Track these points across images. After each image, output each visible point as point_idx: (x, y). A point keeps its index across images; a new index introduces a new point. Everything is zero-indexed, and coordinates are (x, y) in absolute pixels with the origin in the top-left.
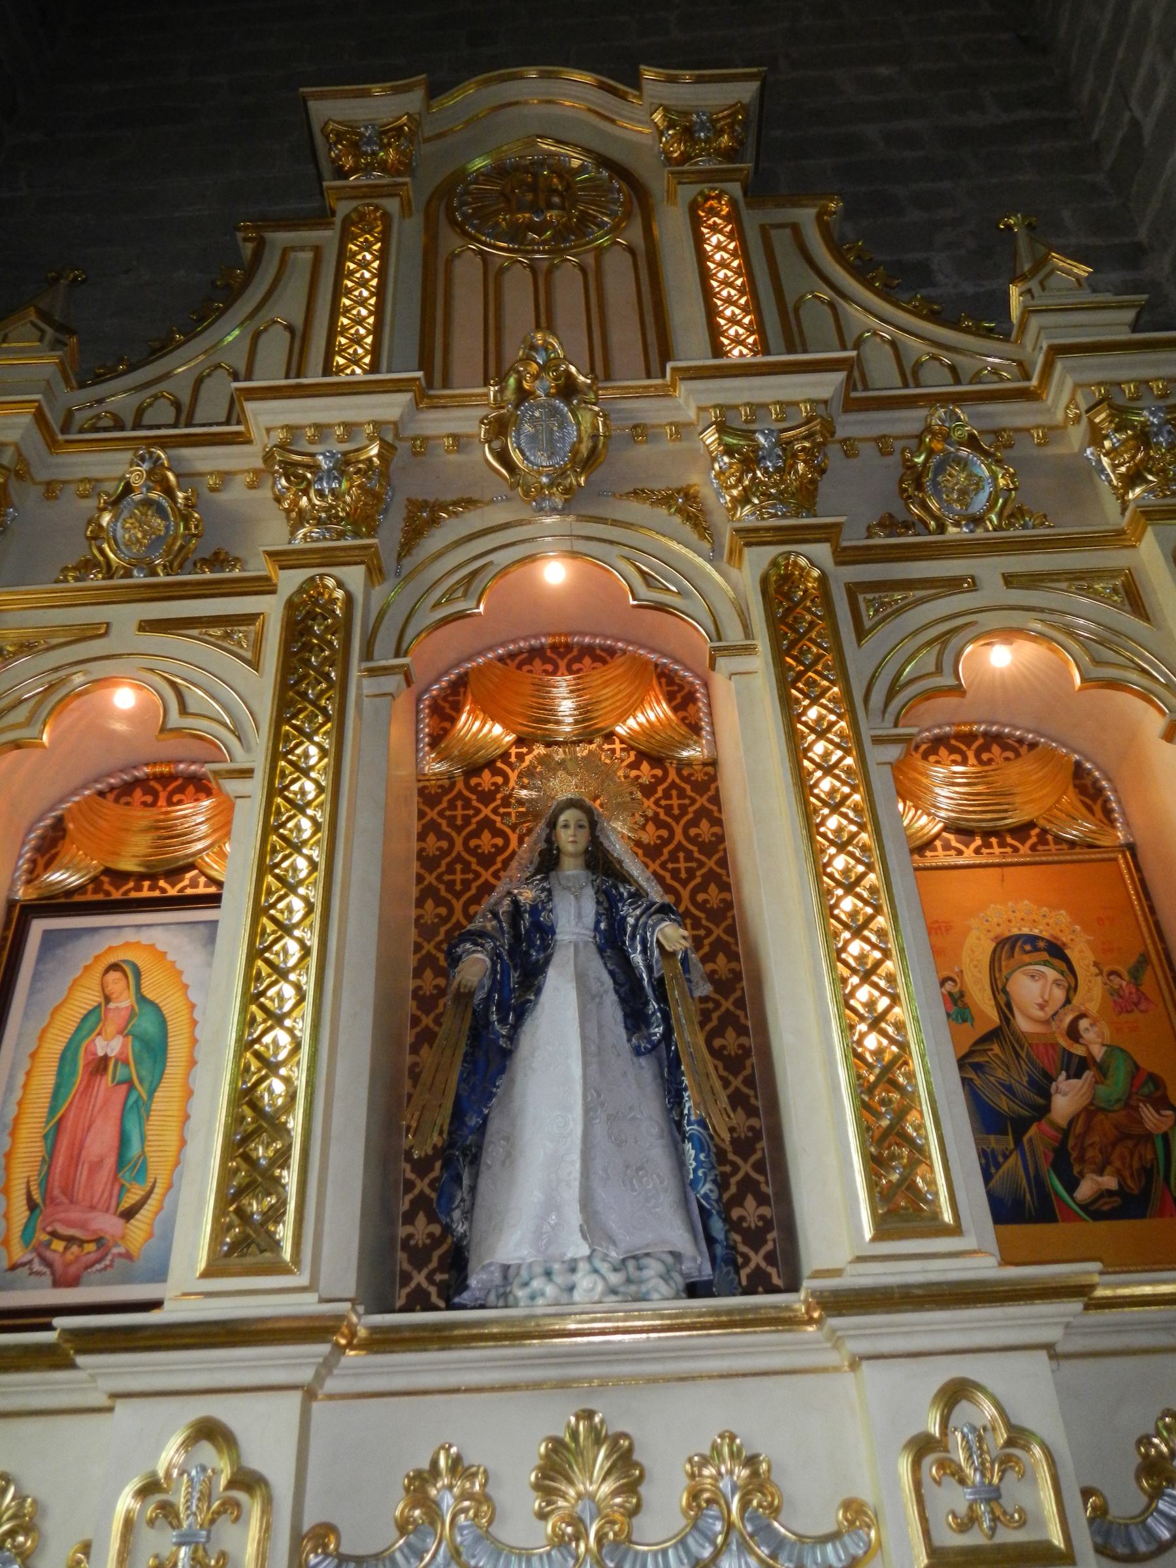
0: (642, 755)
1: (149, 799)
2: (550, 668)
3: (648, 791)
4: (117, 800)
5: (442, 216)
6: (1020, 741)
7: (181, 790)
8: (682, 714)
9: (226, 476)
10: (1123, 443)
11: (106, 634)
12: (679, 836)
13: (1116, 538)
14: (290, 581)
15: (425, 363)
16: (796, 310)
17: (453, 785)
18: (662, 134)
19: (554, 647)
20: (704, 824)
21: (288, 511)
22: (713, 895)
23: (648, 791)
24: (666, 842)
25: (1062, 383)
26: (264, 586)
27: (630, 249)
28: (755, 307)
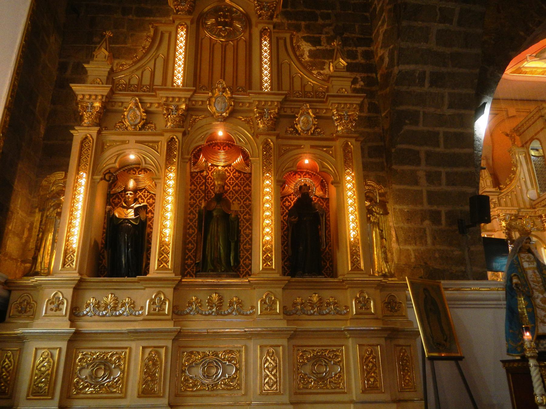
0: (236, 170)
1: (134, 172)
2: (219, 148)
3: (237, 178)
4: (127, 172)
5: (201, 24)
6: (313, 174)
7: (141, 171)
8: (246, 161)
9: (151, 104)
10: (338, 119)
11: (128, 143)
12: (242, 189)
13: (333, 140)
14: (168, 136)
15: (195, 85)
16: (281, 64)
17: (198, 174)
18: (256, 7)
19: (221, 143)
20: (247, 187)
21: (166, 118)
22: (247, 202)
23: (237, 178)
24: (239, 190)
25: (329, 102)
26: (162, 135)
27: (245, 41)
28: (271, 66)
